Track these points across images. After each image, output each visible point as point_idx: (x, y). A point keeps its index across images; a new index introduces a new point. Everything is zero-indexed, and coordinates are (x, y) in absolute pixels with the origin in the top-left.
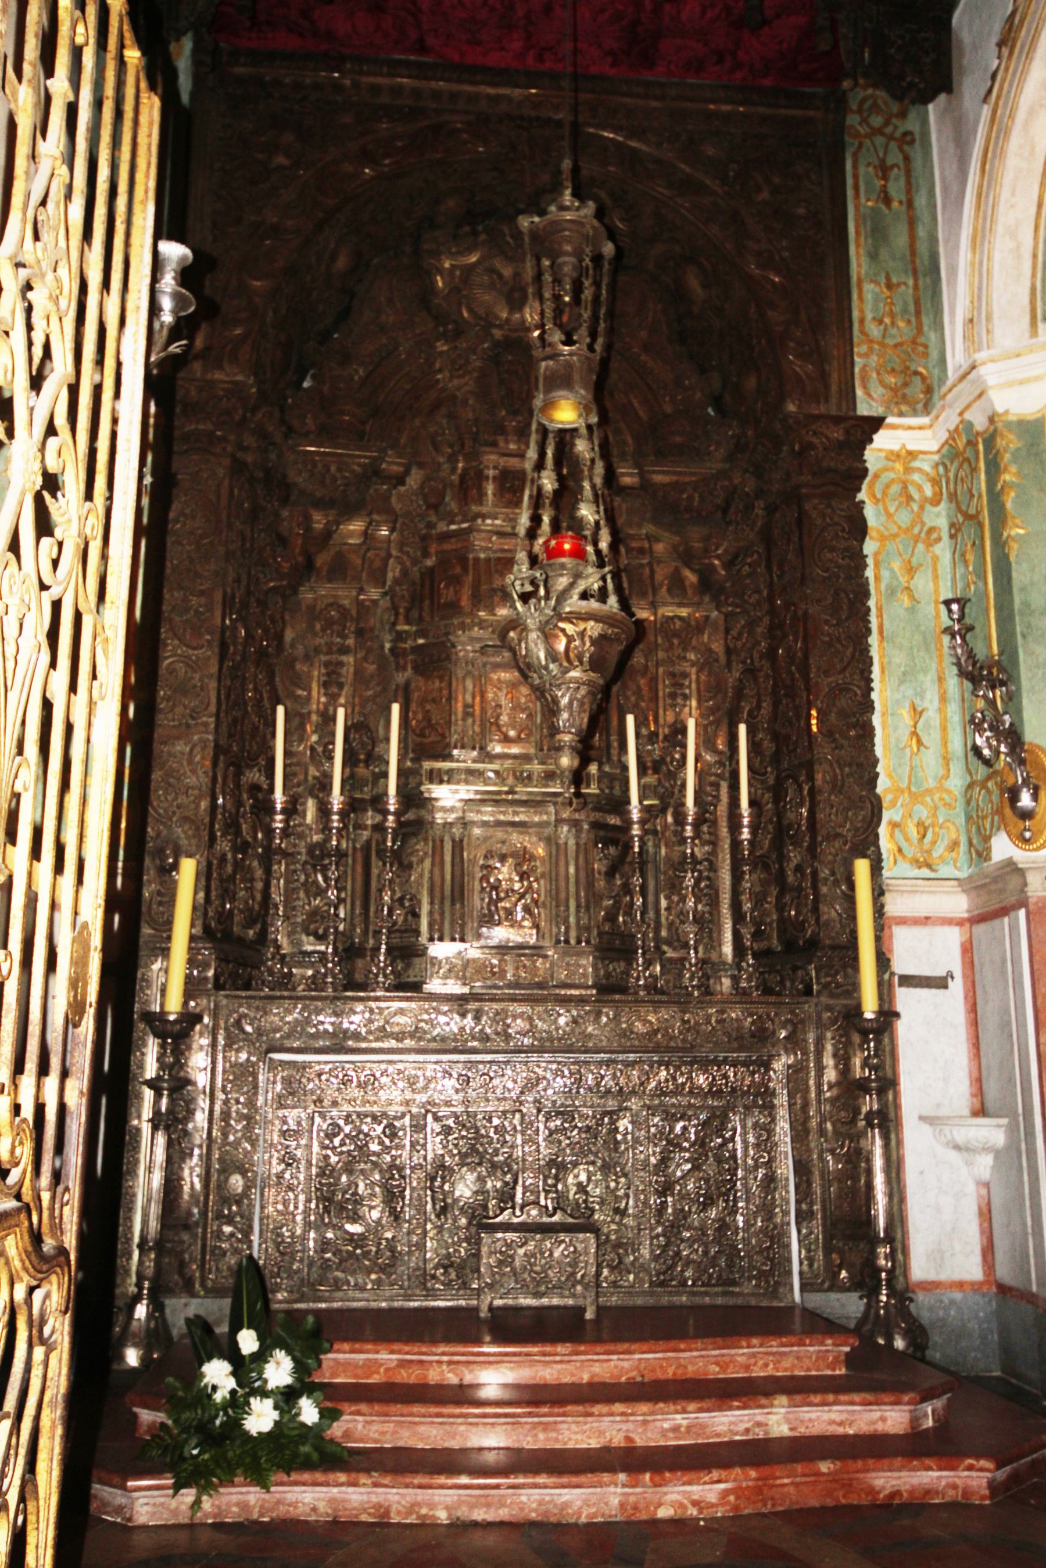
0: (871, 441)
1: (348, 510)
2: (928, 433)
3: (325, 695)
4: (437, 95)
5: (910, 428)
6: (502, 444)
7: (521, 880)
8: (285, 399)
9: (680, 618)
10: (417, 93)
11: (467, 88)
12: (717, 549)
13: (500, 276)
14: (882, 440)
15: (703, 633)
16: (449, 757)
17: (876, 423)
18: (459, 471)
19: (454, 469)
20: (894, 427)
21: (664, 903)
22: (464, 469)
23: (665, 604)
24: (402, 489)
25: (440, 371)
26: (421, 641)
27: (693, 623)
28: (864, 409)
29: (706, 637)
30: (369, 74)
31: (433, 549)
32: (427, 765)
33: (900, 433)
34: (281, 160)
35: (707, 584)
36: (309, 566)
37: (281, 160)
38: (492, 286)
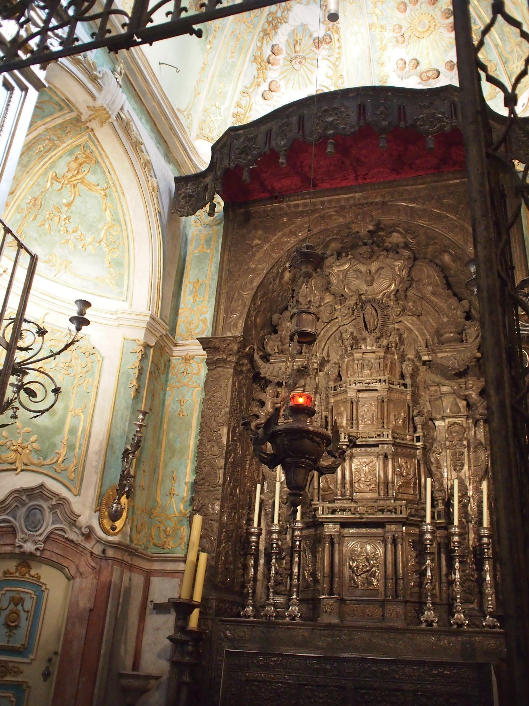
4: (322, 203)
6: (363, 347)
8: (265, 340)
10: (314, 204)
11: (336, 197)
12: (472, 387)
13: (361, 273)
15: (472, 430)
18: (346, 362)
22: (348, 361)
23: (449, 417)
27: (465, 425)
30: (293, 201)
31: (332, 400)
34: (257, 242)
37: (257, 242)
38: (358, 278)
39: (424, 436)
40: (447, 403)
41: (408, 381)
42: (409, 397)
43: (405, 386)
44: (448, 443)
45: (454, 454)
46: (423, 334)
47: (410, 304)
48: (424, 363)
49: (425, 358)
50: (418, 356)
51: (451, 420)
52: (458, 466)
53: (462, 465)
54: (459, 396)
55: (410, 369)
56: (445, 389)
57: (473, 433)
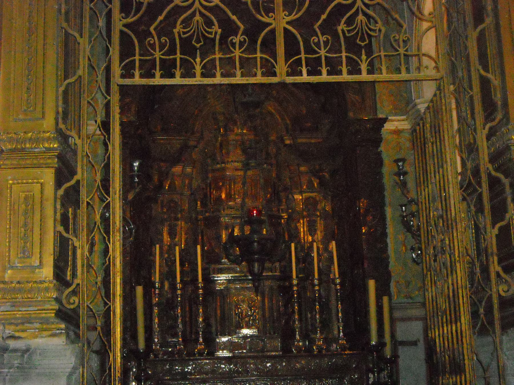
0: (383, 126)
1: (176, 161)
2: (406, 122)
3: (170, 238)
5: (399, 121)
7: (251, 310)
9: (312, 198)
14: (388, 126)
16: (220, 263)
17: (385, 120)
19: (217, 140)
20: (392, 121)
21: (309, 315)
24: (197, 149)
25: (209, 99)
26: (207, 214)
28: (380, 116)
29: (323, 204)
31: (210, 176)
32: (213, 266)
33: (395, 123)
35: (321, 184)
36: (161, 186)
39: (288, 209)
40: (304, 180)
41: (273, 161)
42: (274, 175)
43: (271, 165)
44: (305, 213)
45: (308, 222)
46: (283, 119)
47: (274, 92)
48: (286, 145)
49: (288, 142)
50: (282, 141)
51: (307, 194)
52: (312, 230)
53: (316, 230)
54: (315, 175)
55: (274, 150)
56: (302, 169)
57: (323, 206)
